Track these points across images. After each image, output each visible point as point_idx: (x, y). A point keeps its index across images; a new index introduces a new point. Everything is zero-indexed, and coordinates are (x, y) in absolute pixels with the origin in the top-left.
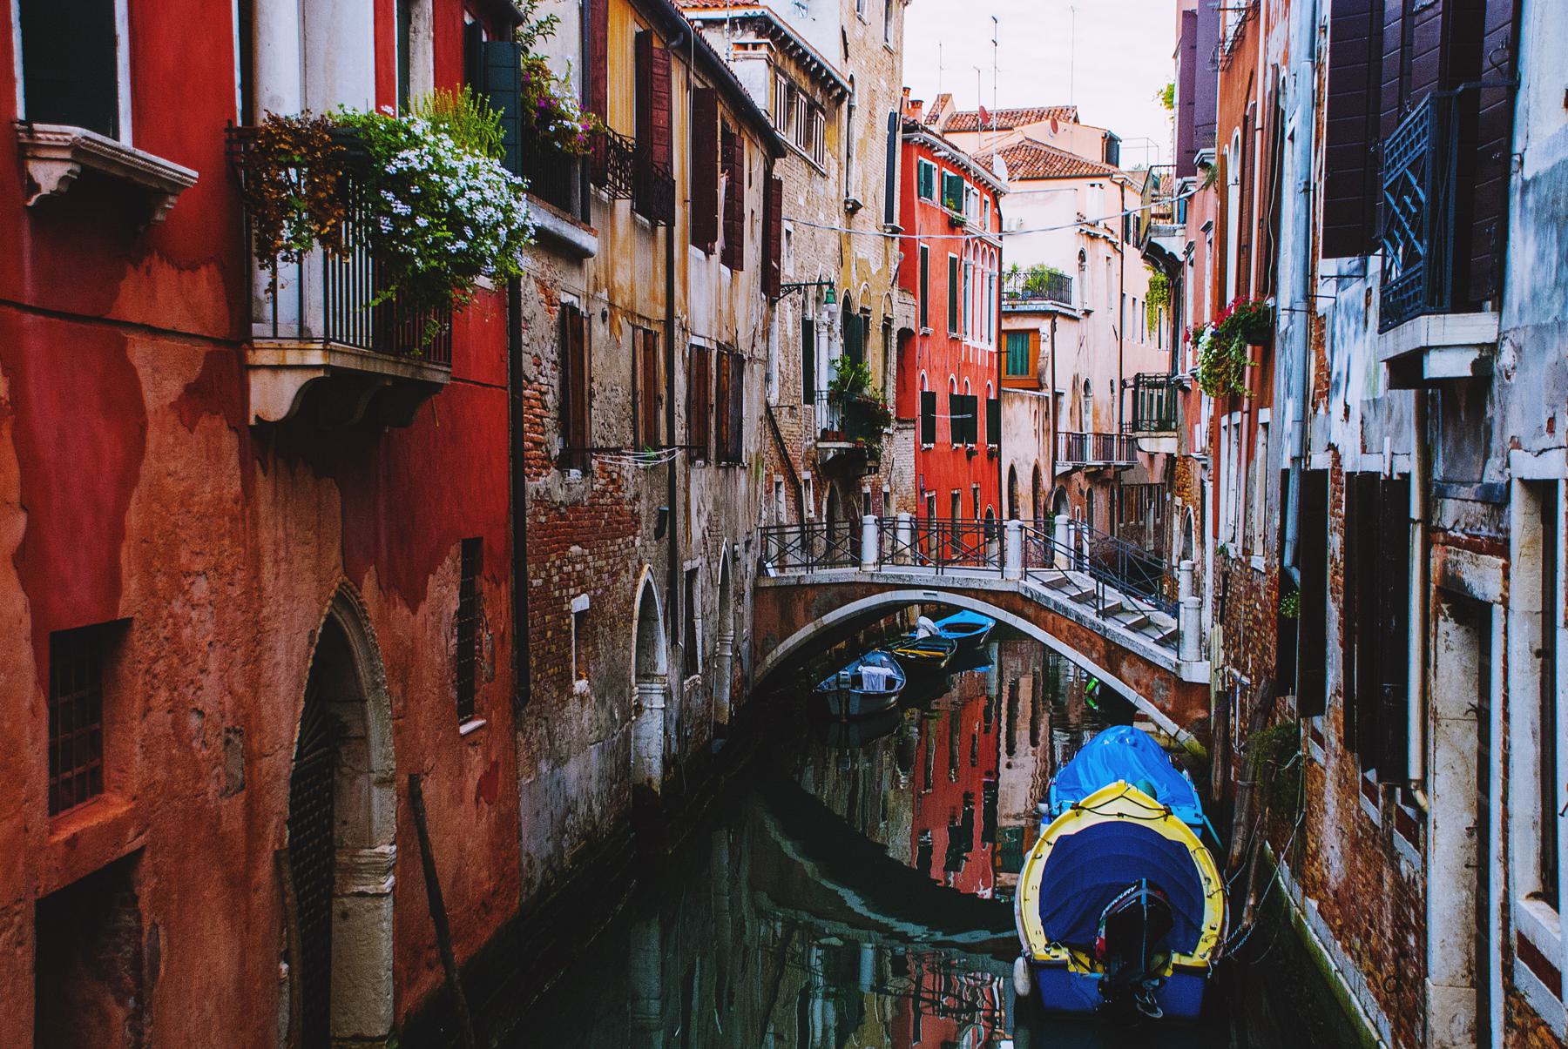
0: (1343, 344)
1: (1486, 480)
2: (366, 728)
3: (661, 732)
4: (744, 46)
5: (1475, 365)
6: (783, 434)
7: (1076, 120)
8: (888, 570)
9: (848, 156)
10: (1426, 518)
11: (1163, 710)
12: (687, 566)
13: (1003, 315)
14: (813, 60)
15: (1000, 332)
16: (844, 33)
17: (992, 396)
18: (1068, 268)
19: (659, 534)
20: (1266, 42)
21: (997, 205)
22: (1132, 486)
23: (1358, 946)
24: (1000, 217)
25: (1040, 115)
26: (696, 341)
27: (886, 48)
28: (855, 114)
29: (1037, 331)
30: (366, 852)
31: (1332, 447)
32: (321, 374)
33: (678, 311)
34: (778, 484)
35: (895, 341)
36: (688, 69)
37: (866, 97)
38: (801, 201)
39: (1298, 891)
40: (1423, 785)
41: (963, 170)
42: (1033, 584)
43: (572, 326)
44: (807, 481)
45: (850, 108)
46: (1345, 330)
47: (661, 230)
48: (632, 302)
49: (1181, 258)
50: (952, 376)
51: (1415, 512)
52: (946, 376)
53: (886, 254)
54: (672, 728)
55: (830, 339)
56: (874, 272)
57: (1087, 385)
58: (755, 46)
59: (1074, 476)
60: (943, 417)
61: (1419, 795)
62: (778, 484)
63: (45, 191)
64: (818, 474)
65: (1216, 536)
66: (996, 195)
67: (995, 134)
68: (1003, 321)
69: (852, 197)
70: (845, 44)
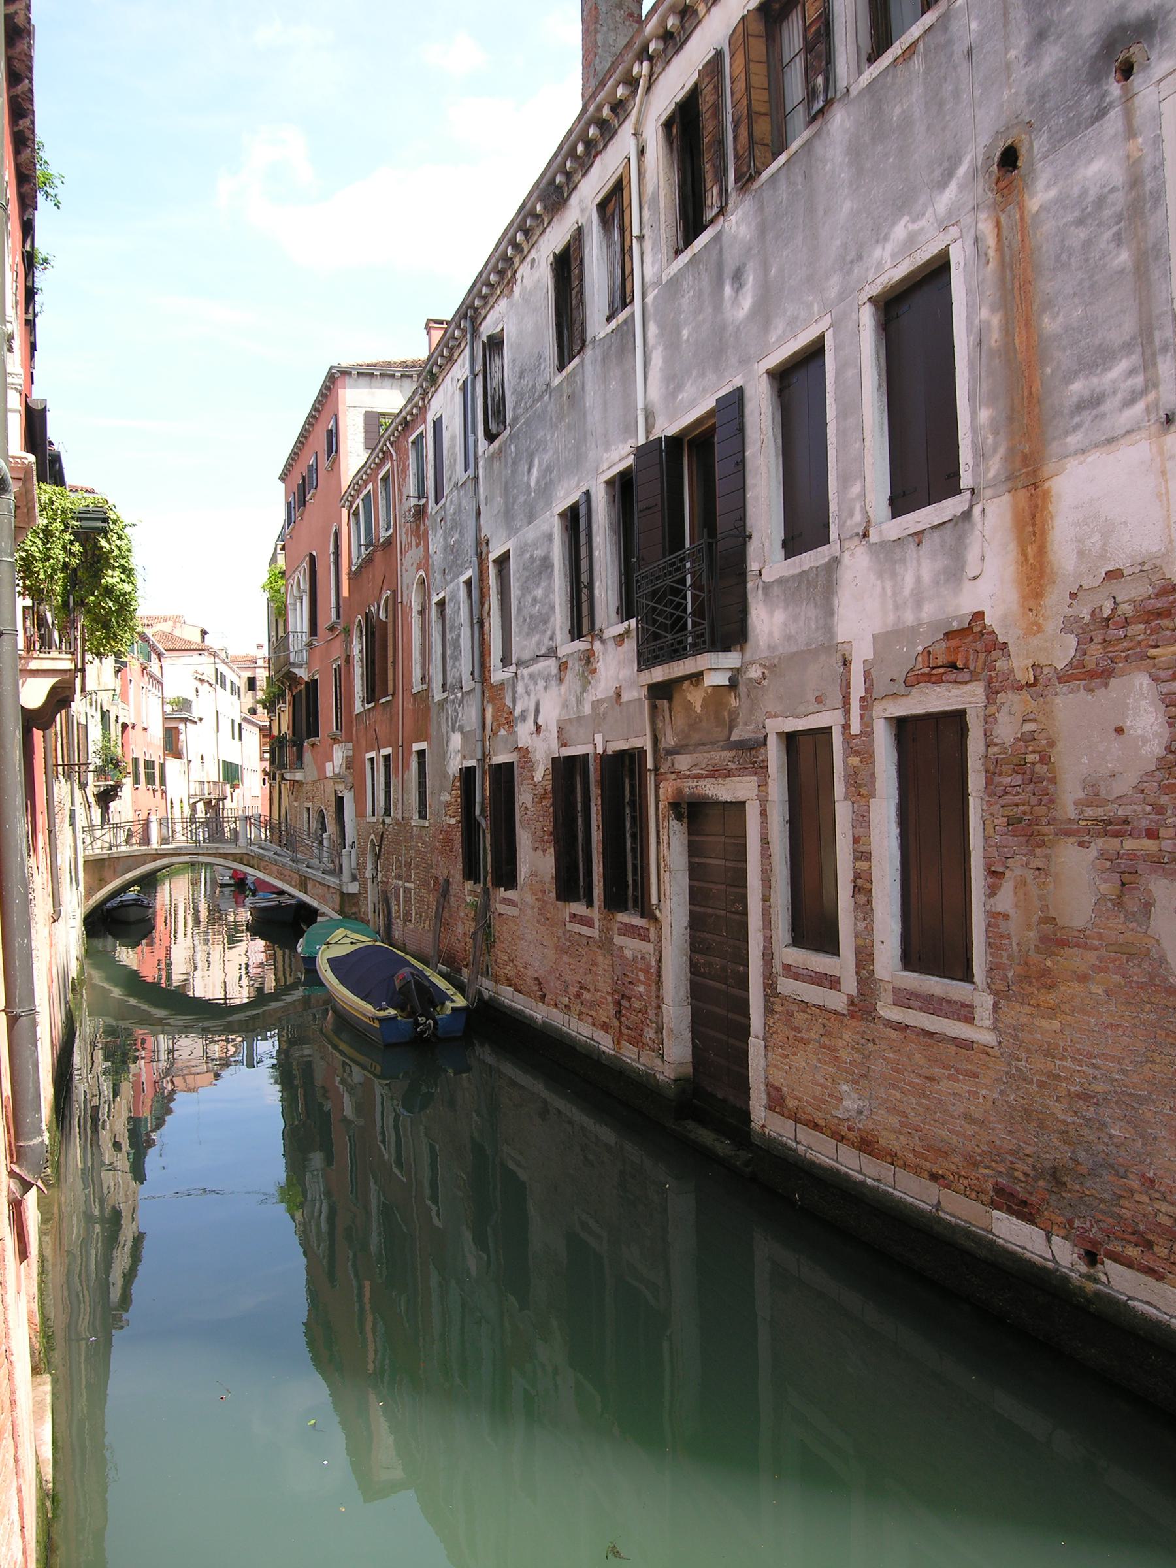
0: (529, 695)
1: (732, 739)
5: (730, 679)
10: (656, 769)
17: (162, 762)
18: (190, 696)
31: (517, 749)
46: (532, 687)
51: (650, 765)
60: (142, 770)
61: (657, 912)
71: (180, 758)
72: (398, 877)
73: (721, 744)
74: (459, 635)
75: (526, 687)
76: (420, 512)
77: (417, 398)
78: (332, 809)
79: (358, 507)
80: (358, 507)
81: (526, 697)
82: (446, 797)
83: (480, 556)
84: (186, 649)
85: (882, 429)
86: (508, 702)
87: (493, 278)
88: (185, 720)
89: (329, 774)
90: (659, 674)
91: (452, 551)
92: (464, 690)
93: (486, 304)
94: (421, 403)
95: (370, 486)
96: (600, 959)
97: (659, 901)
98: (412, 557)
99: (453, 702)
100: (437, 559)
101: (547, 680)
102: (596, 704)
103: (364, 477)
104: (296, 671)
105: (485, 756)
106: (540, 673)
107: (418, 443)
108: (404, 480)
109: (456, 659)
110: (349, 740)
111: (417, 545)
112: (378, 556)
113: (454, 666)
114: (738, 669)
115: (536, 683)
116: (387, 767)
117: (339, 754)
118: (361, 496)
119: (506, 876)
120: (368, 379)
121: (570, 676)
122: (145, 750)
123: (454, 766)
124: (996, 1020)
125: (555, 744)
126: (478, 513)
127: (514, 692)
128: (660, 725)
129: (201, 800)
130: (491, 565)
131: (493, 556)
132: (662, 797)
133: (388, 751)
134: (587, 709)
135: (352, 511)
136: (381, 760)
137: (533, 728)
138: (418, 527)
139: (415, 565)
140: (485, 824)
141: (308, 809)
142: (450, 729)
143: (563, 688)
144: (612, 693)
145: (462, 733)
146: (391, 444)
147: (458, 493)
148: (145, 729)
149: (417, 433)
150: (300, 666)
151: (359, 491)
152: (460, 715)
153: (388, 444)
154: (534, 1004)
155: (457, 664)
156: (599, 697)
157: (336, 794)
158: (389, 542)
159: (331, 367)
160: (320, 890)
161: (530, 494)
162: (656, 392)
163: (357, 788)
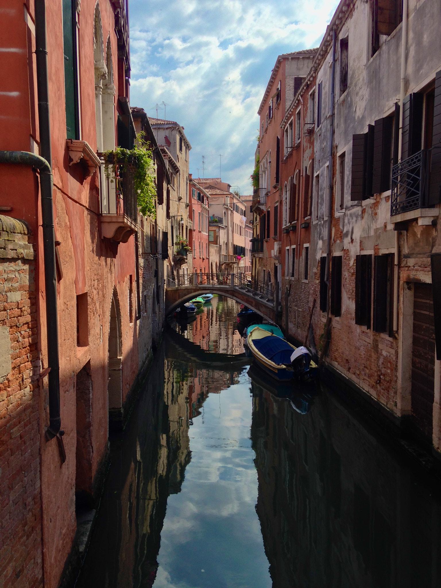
0: (349, 224)
5: (432, 221)
9: (179, 186)
11: (270, 318)
20: (303, 154)
27: (186, 160)
28: (180, 176)
29: (215, 230)
31: (343, 250)
35: (188, 232)
40: (397, 332)
46: (351, 220)
51: (396, 262)
61: (396, 335)
63: (74, 162)
68: (210, 227)
71: (216, 244)
73: (428, 254)
74: (324, 193)
75: (349, 220)
76: (311, 132)
77: (312, 72)
78: (273, 271)
79: (287, 128)
80: (287, 128)
81: (348, 225)
82: (315, 270)
83: (333, 155)
86: (341, 227)
89: (273, 255)
90: (399, 218)
91: (323, 151)
92: (324, 220)
94: (314, 75)
95: (292, 118)
96: (373, 354)
97: (398, 329)
98: (308, 153)
99: (320, 225)
100: (317, 156)
101: (357, 217)
102: (376, 230)
103: (290, 113)
104: (261, 207)
105: (330, 252)
106: (354, 213)
107: (313, 95)
108: (306, 114)
109: (322, 204)
110: (280, 240)
111: (310, 148)
112: (294, 152)
113: (321, 208)
114: (437, 216)
115: (352, 219)
116: (294, 254)
117: (276, 246)
118: (289, 122)
119: (337, 311)
120: (297, 60)
121: (366, 216)
123: (318, 257)
125: (358, 248)
126: (333, 132)
127: (344, 222)
128: (402, 242)
130: (338, 158)
131: (339, 154)
132: (401, 279)
133: (294, 246)
134: (372, 233)
135: (285, 130)
136: (292, 250)
137: (350, 240)
138: (310, 138)
139: (309, 157)
140: (329, 284)
141: (264, 270)
142: (318, 239)
143: (364, 221)
144: (383, 225)
145: (323, 240)
146: (302, 96)
147: (327, 122)
149: (312, 91)
150: (263, 204)
151: (288, 120)
152: (322, 232)
153: (300, 96)
154: (346, 372)
155: (322, 207)
156: (378, 227)
157: (275, 265)
158: (299, 145)
159: (279, 56)
160: (263, 309)
161: (355, 123)
162: (410, 70)
163: (282, 263)
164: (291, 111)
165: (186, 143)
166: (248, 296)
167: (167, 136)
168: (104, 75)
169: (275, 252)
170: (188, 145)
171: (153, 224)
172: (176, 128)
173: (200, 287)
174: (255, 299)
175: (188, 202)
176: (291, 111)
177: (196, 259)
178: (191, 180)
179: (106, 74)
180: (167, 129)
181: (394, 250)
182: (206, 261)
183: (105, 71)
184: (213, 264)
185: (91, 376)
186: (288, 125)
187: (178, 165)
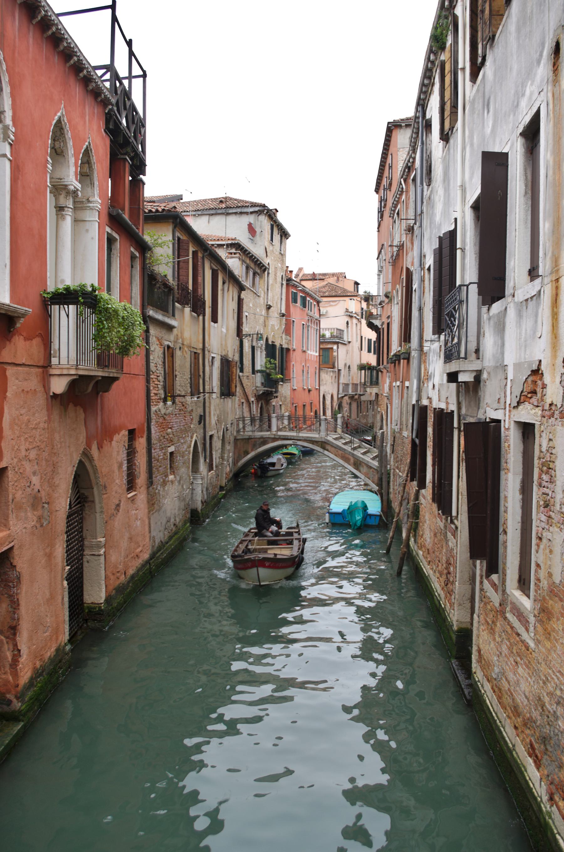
1: (478, 417)
2: (94, 497)
3: (201, 492)
4: (231, 253)
5: (475, 377)
6: (244, 385)
7: (345, 277)
8: (280, 433)
9: (268, 290)
11: (373, 482)
12: (211, 433)
13: (321, 343)
14: (255, 258)
15: (320, 349)
16: (266, 248)
18: (343, 327)
19: (200, 423)
20: (406, 258)
21: (318, 306)
22: (364, 401)
23: (434, 568)
24: (320, 310)
25: (333, 275)
26: (213, 355)
27: (280, 253)
28: (270, 275)
29: (332, 348)
30: (94, 540)
31: (428, 398)
32: (75, 377)
33: (207, 345)
34: (243, 403)
36: (211, 262)
37: (273, 270)
38: (251, 305)
39: (416, 547)
41: (308, 294)
42: (329, 438)
43: (169, 352)
44: (253, 402)
45: (268, 273)
47: (201, 318)
48: (190, 343)
49: (380, 327)
50: (303, 364)
52: (301, 364)
53: (281, 323)
54: (205, 489)
55: (261, 352)
56: (276, 329)
57: (349, 367)
58: (235, 254)
59: (345, 398)
61: (455, 521)
62: (243, 403)
64: (257, 399)
65: (391, 423)
66: (318, 302)
67: (318, 281)
69: (269, 303)
70: (266, 252)
72: (397, 468)
84: (344, 294)
85: (526, 222)
87: (426, 82)
88: (337, 343)
93: (426, 97)
94: (413, 156)
95: (399, 206)
105: (419, 400)
114: (481, 371)
118: (397, 211)
122: (303, 364)
124: (535, 635)
129: (346, 395)
131: (427, 267)
148: (304, 352)
150: (376, 318)
151: (395, 207)
159: (389, 123)
164: (396, 197)
165: (282, 230)
166: (345, 450)
167: (252, 222)
168: (75, 192)
169: (386, 387)
170: (284, 232)
171: (199, 351)
172: (264, 211)
173: (280, 436)
174: (353, 454)
175: (283, 311)
176: (396, 197)
177: (296, 392)
178: (289, 280)
179: (78, 190)
180: (252, 213)
181: (453, 407)
182: (314, 393)
183: (75, 187)
184: (326, 397)
185: (15, 566)
186: (396, 215)
187: (266, 261)
